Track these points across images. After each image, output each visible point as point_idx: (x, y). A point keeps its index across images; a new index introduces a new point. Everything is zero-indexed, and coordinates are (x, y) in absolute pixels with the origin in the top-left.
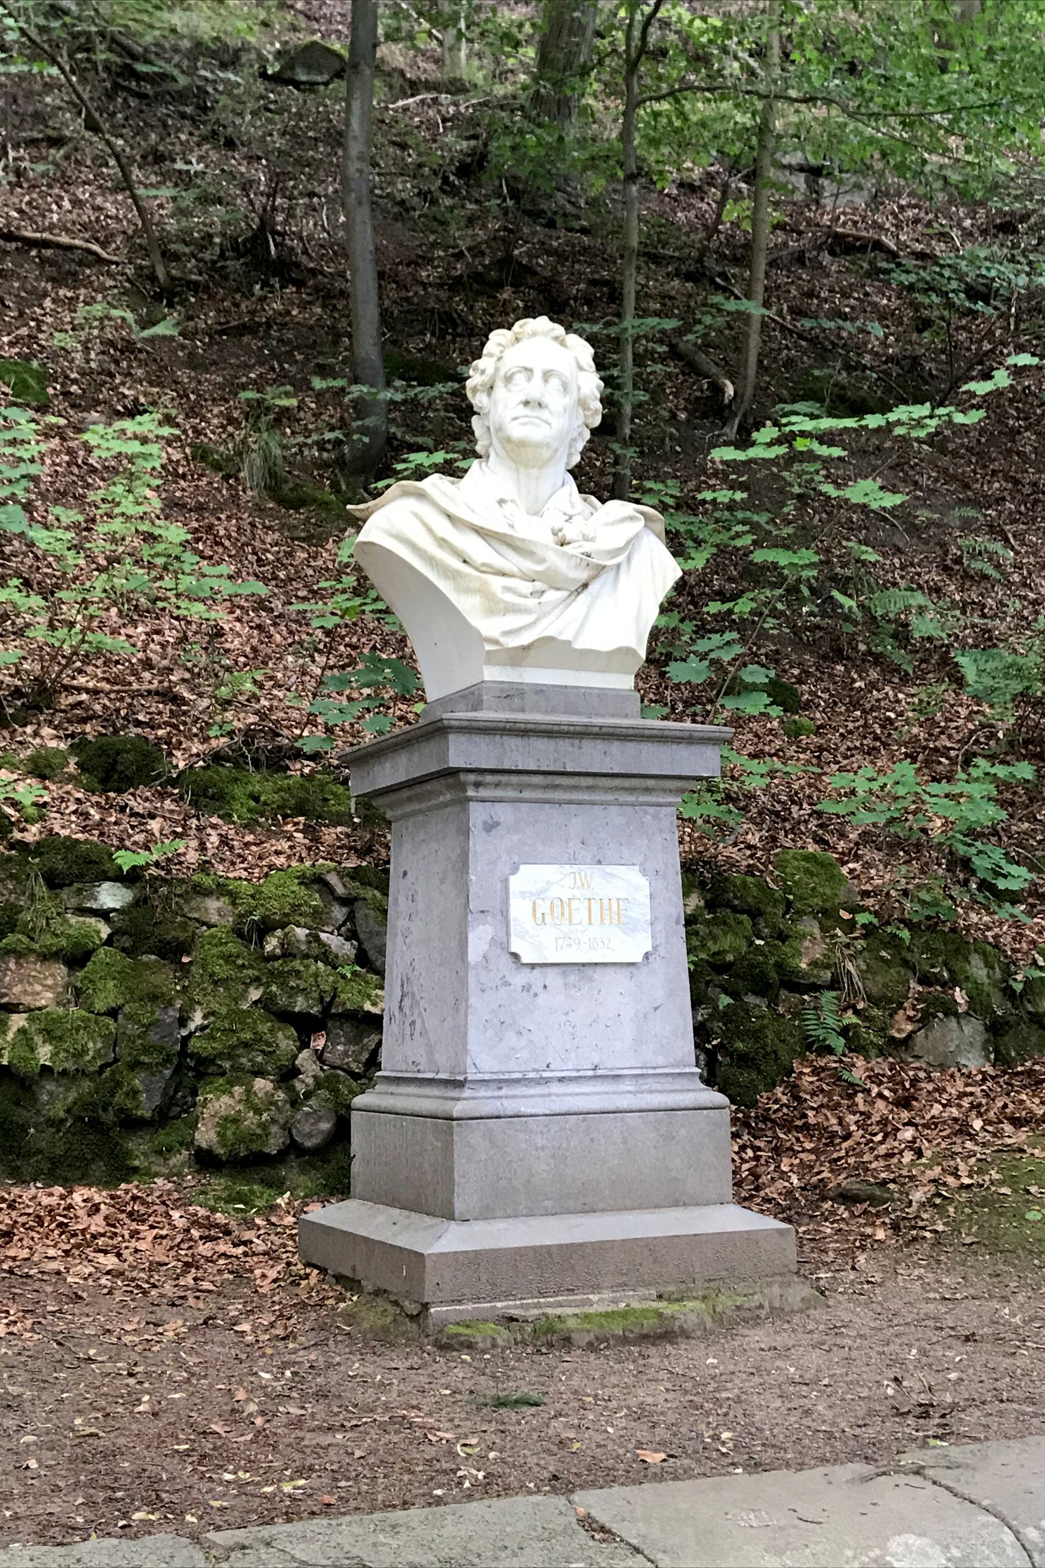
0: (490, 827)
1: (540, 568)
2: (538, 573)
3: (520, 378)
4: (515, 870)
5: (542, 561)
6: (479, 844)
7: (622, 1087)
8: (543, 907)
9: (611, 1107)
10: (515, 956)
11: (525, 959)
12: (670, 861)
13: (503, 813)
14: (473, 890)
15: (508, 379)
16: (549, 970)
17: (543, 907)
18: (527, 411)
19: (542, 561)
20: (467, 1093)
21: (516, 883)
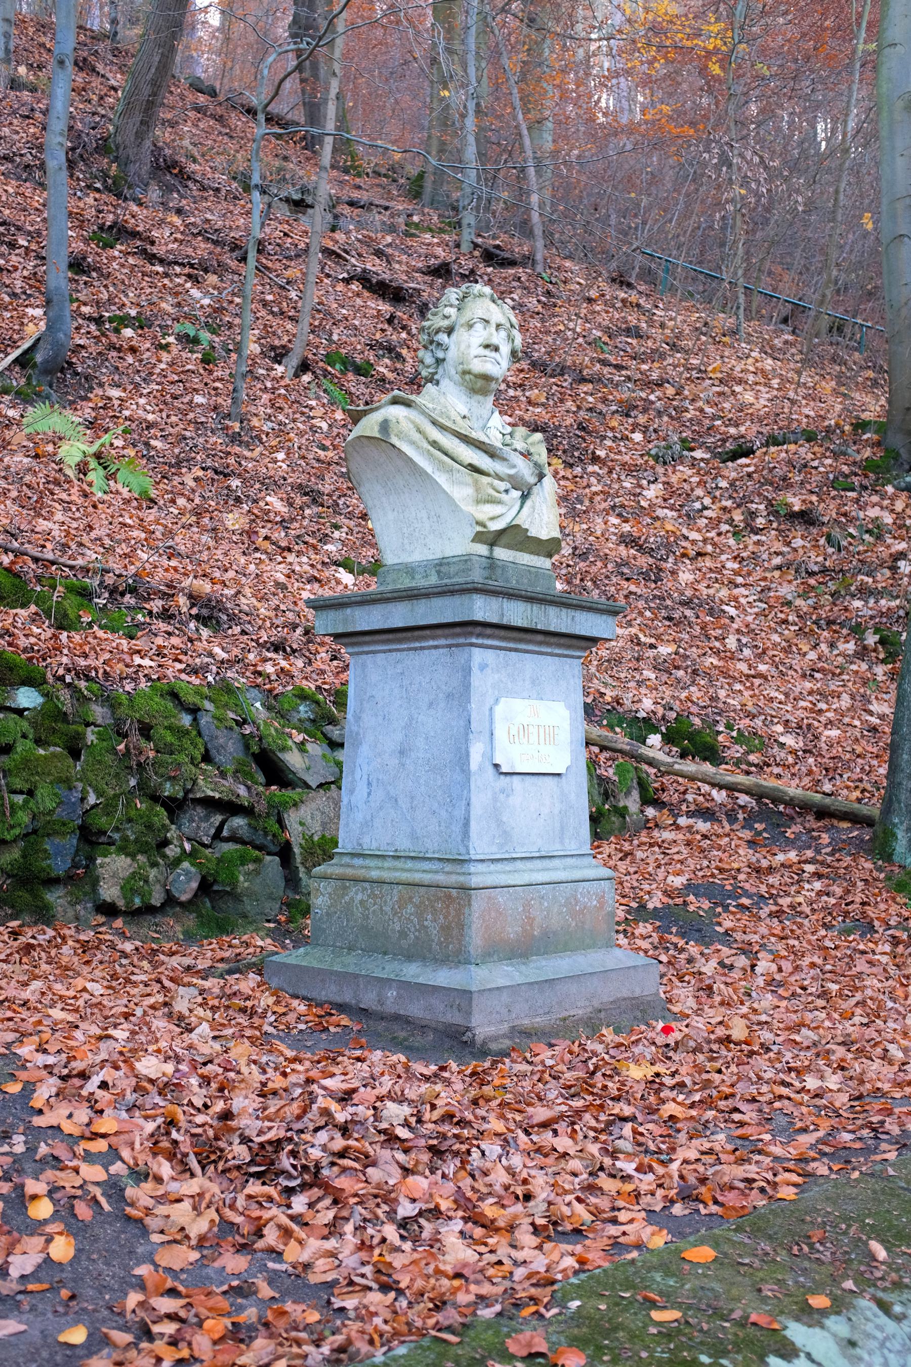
0: (483, 667)
1: (512, 472)
2: (510, 476)
3: (479, 326)
4: (497, 701)
5: (514, 466)
6: (476, 679)
7: (386, 864)
8: (514, 731)
9: (556, 879)
10: (496, 766)
11: (504, 770)
12: (579, 700)
13: (490, 655)
14: (474, 717)
15: (470, 326)
16: (515, 777)
17: (514, 731)
18: (487, 352)
19: (514, 466)
20: (472, 868)
21: (499, 710)
